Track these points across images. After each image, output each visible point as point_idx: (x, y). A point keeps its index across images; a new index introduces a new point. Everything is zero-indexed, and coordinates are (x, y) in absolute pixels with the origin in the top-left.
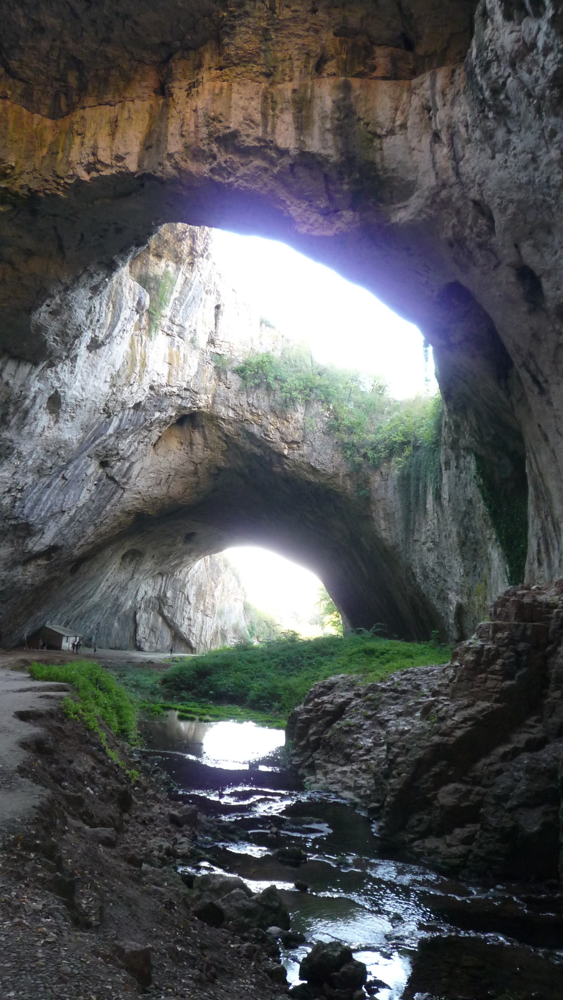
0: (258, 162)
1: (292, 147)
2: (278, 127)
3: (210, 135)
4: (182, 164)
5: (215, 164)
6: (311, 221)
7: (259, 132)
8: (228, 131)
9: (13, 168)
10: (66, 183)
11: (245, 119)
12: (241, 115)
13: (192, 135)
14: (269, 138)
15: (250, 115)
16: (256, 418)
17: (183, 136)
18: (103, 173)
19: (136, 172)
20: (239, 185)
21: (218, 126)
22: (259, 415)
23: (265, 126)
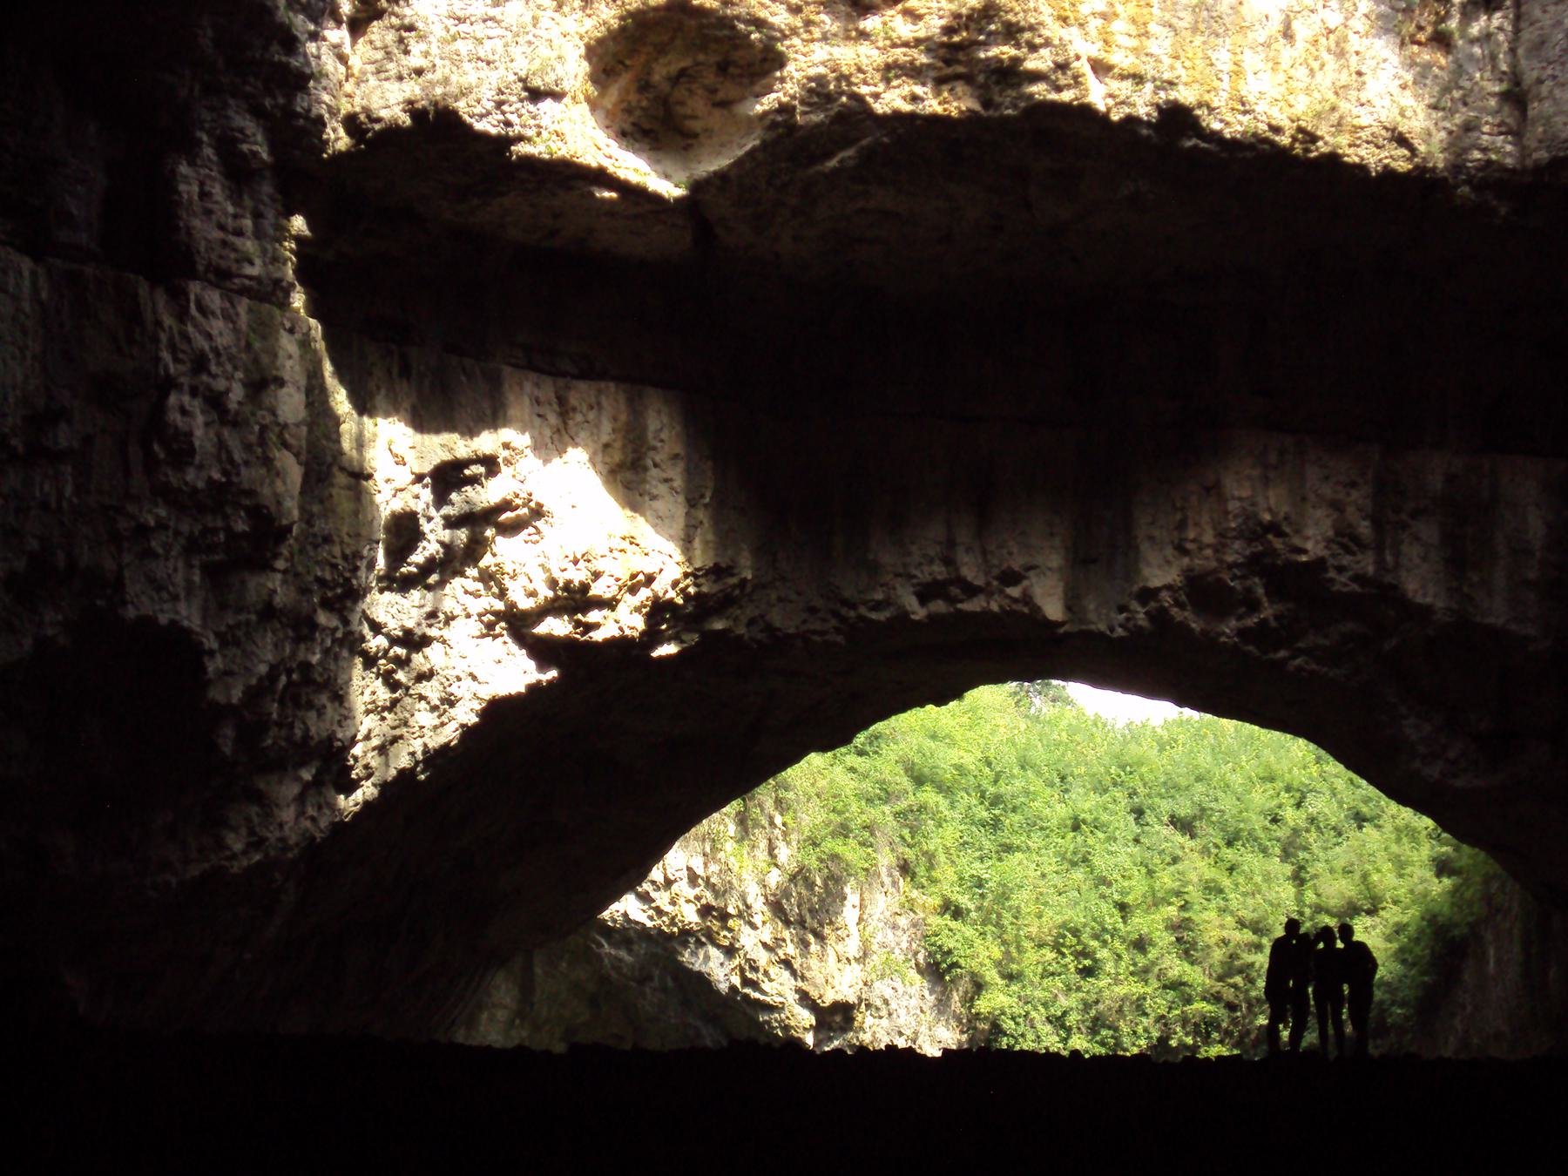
0: (1349, 626)
1: (1440, 604)
2: (1405, 548)
3: (1254, 564)
4: (1174, 611)
5: (1251, 621)
6: (1452, 755)
7: (1367, 564)
8: (1304, 558)
9: (744, 582)
10: (861, 618)
11: (1338, 533)
12: (1329, 522)
13: (1209, 552)
14: (1388, 579)
15: (1350, 526)
16: (715, 925)
17: (1182, 550)
18: (967, 606)
19: (1062, 624)
20: (1299, 669)
21: (1278, 544)
22: (724, 917)
23: (1380, 549)
